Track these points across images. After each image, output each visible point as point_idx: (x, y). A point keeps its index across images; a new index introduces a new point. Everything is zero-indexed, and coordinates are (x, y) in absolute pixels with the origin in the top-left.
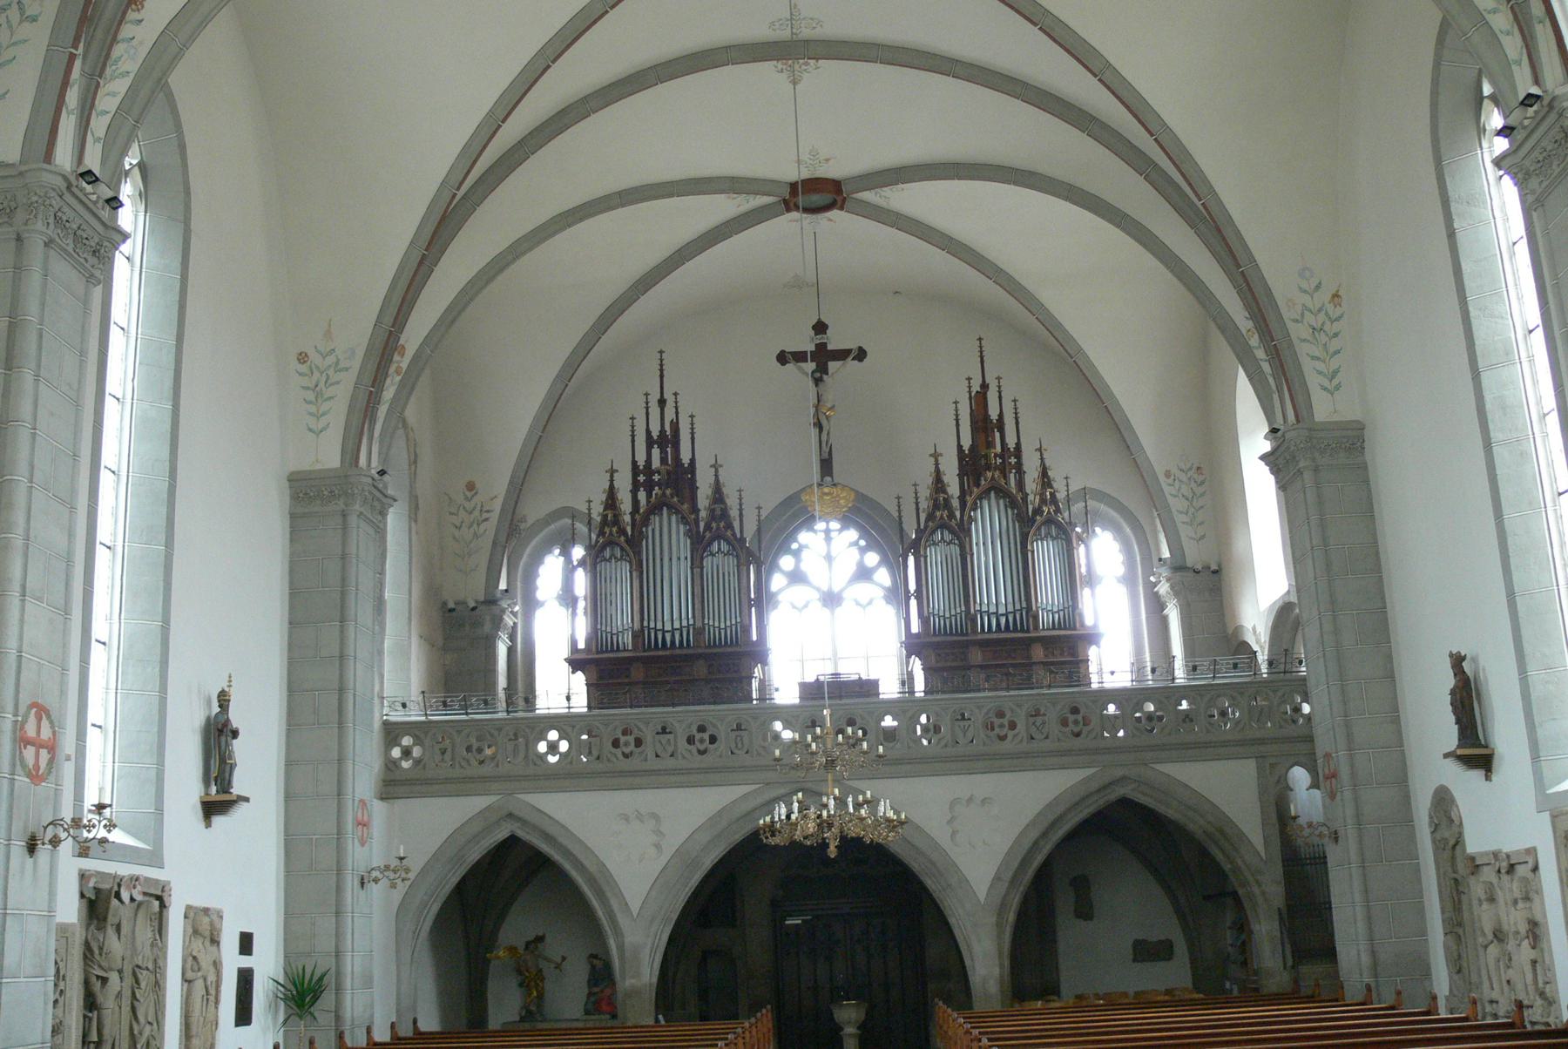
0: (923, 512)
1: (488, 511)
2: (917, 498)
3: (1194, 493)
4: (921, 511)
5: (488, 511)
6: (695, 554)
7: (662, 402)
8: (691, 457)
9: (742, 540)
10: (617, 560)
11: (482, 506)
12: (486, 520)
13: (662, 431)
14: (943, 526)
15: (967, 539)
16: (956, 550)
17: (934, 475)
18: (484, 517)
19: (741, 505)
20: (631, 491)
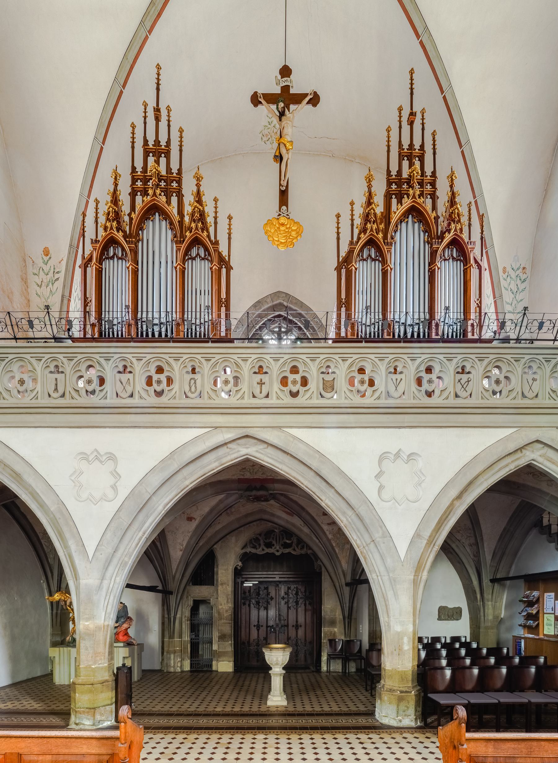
1: (58, 273)
2: (352, 215)
5: (58, 273)
6: (178, 252)
11: (54, 269)
12: (58, 279)
13: (157, 142)
17: (367, 194)
18: (56, 277)
20: (130, 194)
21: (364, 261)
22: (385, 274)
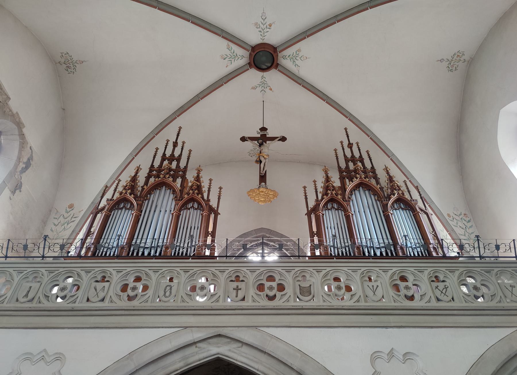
0: (320, 193)
3: (466, 226)
4: (318, 193)
7: (175, 144)
8: (185, 165)
9: (208, 200)
10: (126, 209)
14: (332, 200)
15: (349, 206)
16: (341, 213)
19: (210, 186)
21: (329, 210)
22: (348, 219)
